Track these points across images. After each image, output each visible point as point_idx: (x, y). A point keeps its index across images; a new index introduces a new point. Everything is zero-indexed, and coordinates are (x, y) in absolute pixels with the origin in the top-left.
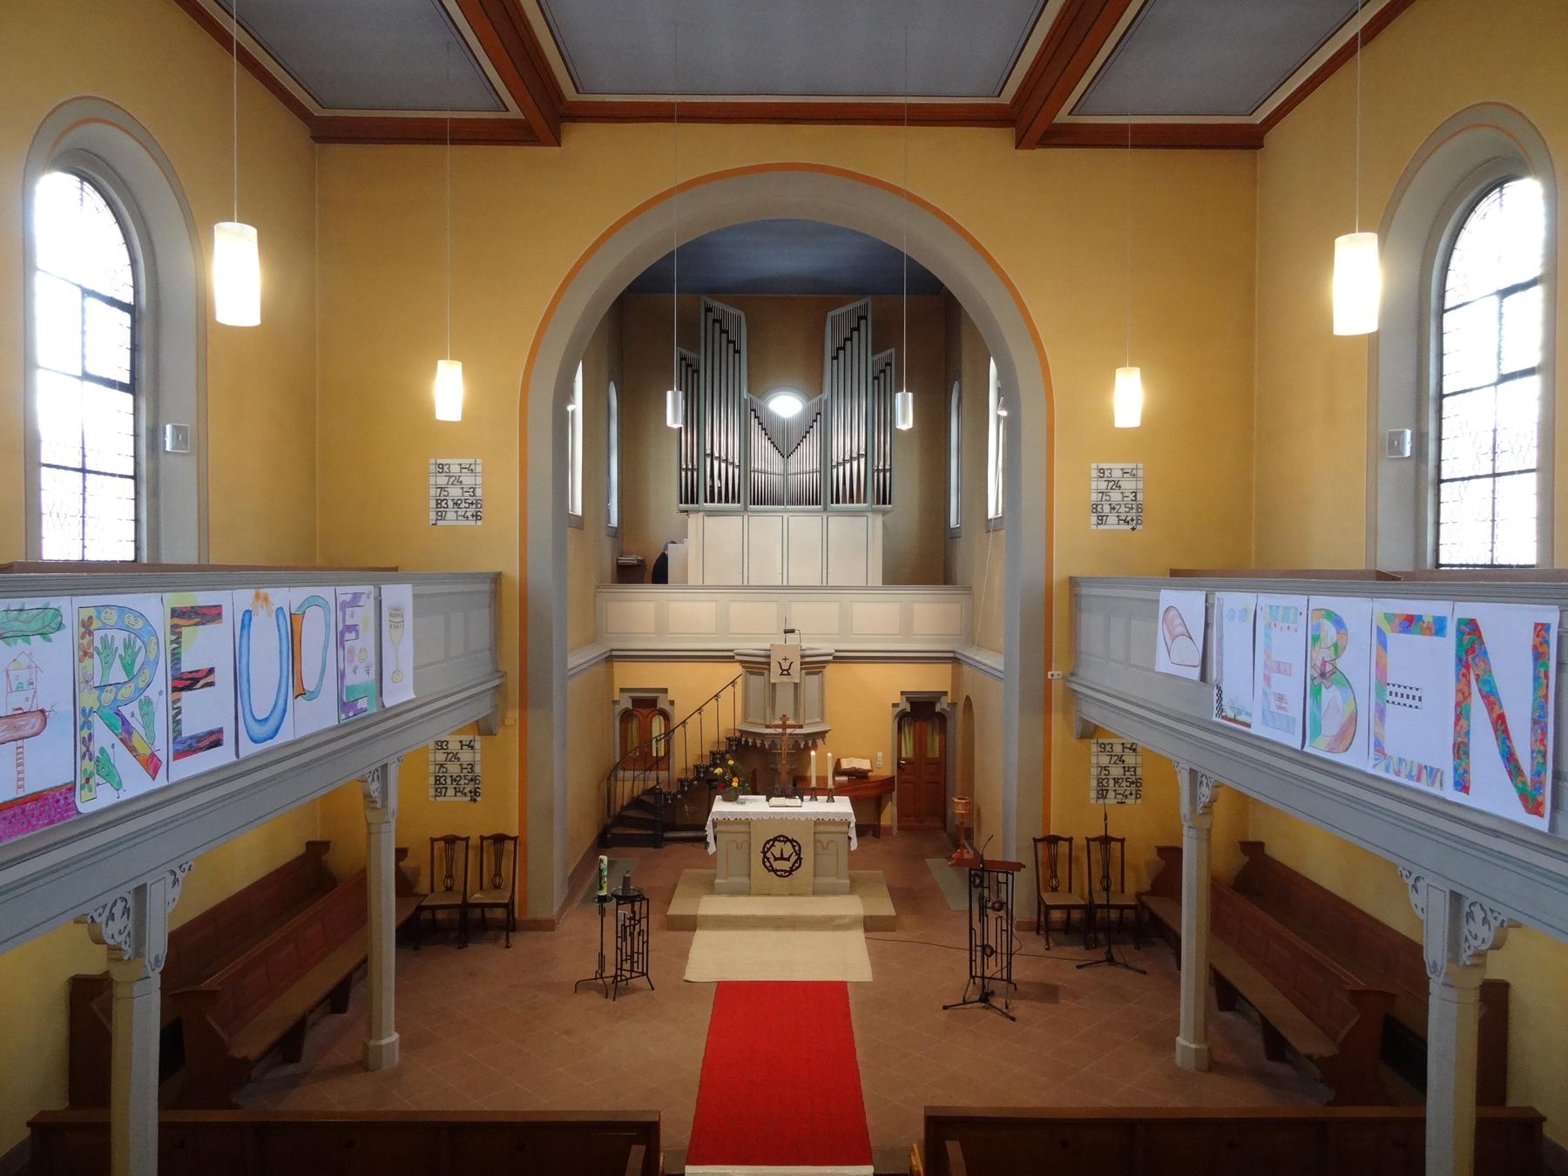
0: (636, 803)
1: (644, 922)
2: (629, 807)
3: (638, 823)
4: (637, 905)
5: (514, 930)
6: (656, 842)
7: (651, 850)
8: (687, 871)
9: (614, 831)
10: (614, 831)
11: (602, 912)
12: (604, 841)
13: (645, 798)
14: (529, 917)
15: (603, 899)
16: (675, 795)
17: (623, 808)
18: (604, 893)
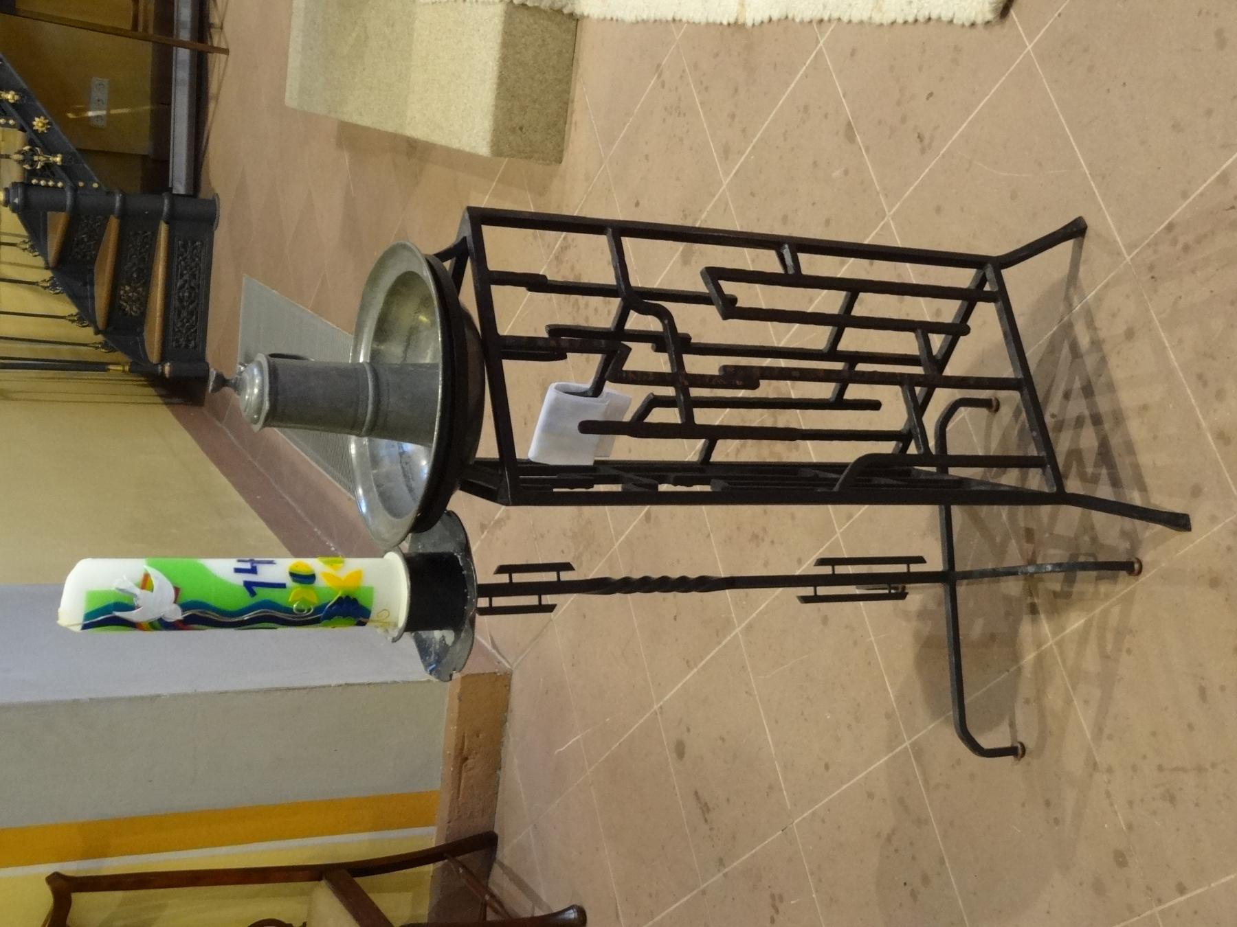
0: (70, 272)
1: (656, 266)
2: (82, 299)
3: (132, 270)
4: (519, 314)
5: (487, 843)
6: (197, 220)
7: (221, 236)
8: (292, 98)
9: (154, 355)
10: (154, 355)
11: (537, 587)
12: (186, 385)
13: (53, 243)
14: (435, 778)
15: (443, 591)
16: (36, 141)
17: (85, 316)
18: (389, 582)
